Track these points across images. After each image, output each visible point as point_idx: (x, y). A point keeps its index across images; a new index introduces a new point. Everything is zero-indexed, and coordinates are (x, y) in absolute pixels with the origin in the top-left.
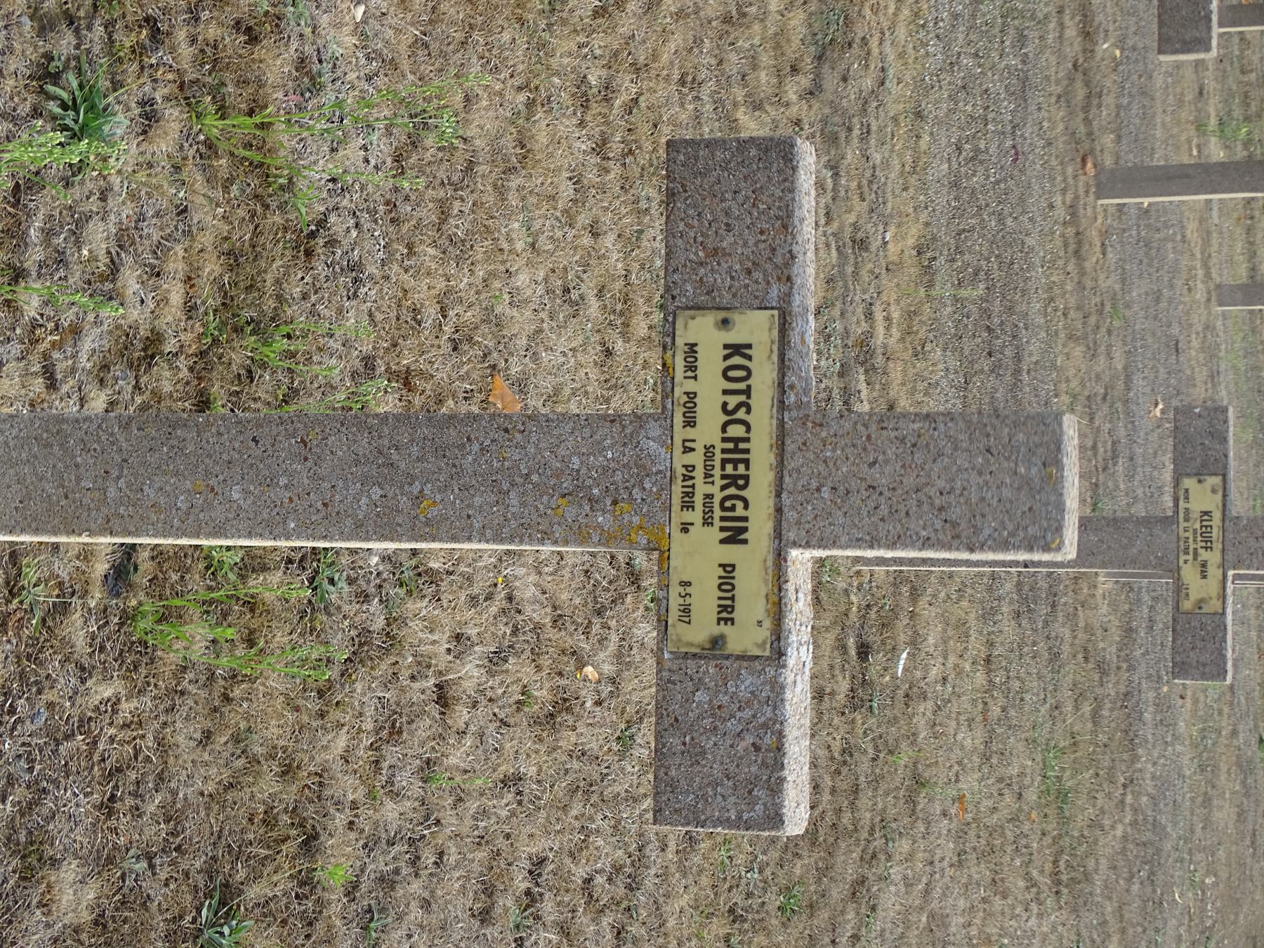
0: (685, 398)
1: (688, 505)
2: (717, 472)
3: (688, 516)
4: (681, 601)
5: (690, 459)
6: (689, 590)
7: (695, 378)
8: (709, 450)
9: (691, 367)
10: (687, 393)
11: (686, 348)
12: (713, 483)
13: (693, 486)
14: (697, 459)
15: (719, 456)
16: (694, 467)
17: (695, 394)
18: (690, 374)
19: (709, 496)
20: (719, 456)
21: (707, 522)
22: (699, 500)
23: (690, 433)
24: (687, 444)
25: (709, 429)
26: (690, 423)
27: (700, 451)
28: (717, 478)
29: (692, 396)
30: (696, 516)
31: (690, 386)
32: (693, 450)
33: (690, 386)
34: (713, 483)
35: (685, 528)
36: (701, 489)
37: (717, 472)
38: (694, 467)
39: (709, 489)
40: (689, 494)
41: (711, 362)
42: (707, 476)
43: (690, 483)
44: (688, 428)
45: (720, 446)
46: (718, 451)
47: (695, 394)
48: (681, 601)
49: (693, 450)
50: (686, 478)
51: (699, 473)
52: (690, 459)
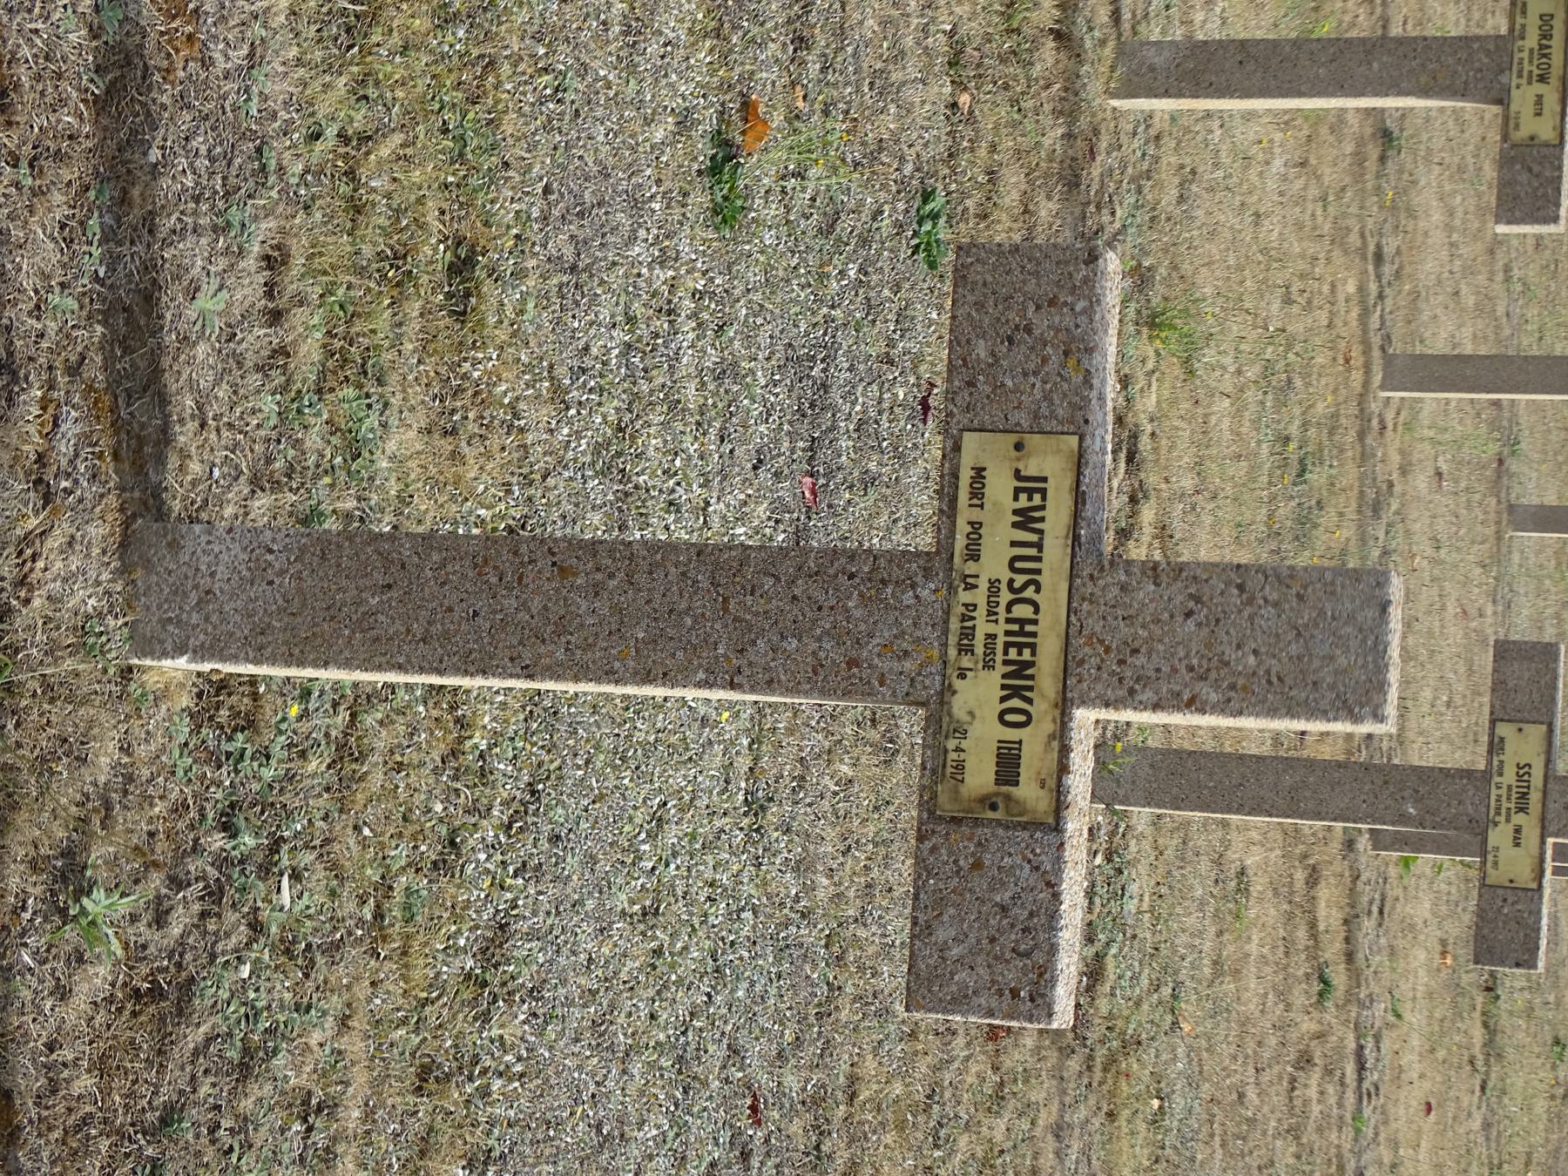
0: (969, 529)
2: (1001, 609)
3: (966, 662)
7: (982, 506)
8: (994, 584)
9: (977, 493)
11: (972, 473)
12: (996, 621)
15: (1005, 596)
16: (975, 606)
17: (981, 524)
18: (975, 501)
23: (971, 567)
24: (969, 580)
25: (994, 564)
26: (974, 556)
27: (983, 585)
29: (976, 526)
31: (976, 515)
33: (976, 515)
34: (996, 621)
36: (982, 628)
37: (1001, 609)
38: (975, 606)
39: (991, 628)
40: (968, 633)
41: (1000, 487)
42: (990, 613)
44: (971, 563)
46: (1004, 586)
47: (981, 524)
49: (976, 587)
50: (964, 618)
51: (981, 613)
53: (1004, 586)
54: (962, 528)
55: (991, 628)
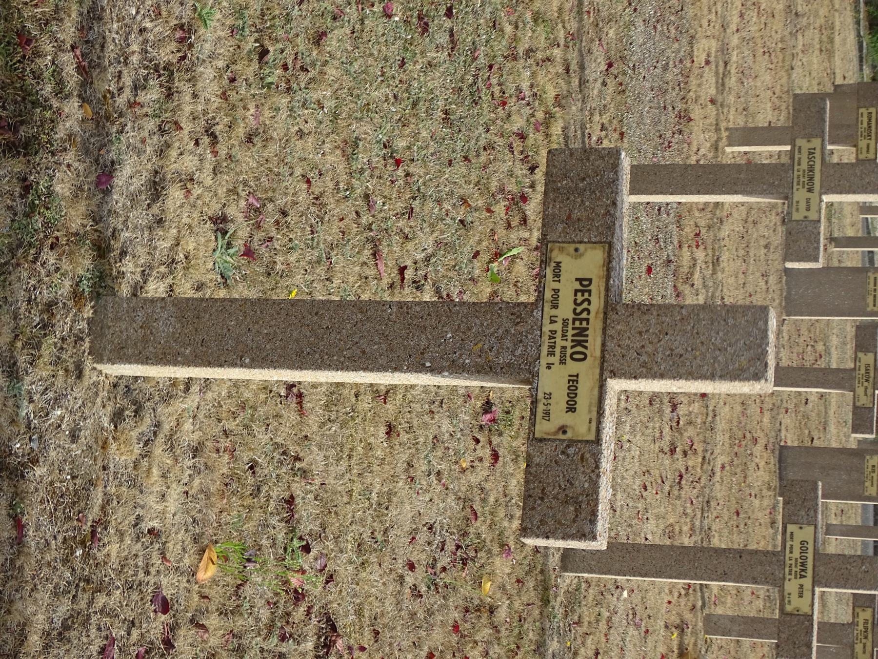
1: (551, 353)
3: (551, 359)
4: (545, 408)
5: (553, 327)
6: (549, 401)
7: (559, 281)
8: (565, 322)
10: (554, 290)
11: (554, 264)
13: (555, 343)
14: (558, 327)
15: (570, 326)
19: (564, 348)
20: (570, 326)
21: (562, 362)
22: (558, 350)
23: (554, 312)
26: (555, 306)
27: (560, 322)
28: (570, 338)
29: (556, 291)
30: (556, 359)
31: (556, 285)
32: (556, 322)
35: (549, 367)
36: (560, 342)
39: (564, 343)
40: (552, 347)
42: (563, 336)
43: (553, 340)
45: (571, 316)
48: (545, 408)
49: (556, 322)
50: (550, 338)
52: (553, 327)
53: (570, 322)
54: (548, 295)
55: (564, 343)
